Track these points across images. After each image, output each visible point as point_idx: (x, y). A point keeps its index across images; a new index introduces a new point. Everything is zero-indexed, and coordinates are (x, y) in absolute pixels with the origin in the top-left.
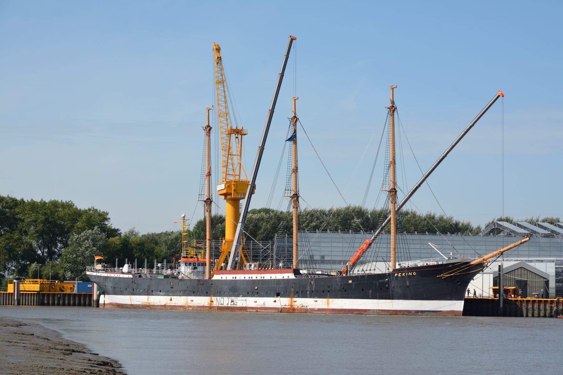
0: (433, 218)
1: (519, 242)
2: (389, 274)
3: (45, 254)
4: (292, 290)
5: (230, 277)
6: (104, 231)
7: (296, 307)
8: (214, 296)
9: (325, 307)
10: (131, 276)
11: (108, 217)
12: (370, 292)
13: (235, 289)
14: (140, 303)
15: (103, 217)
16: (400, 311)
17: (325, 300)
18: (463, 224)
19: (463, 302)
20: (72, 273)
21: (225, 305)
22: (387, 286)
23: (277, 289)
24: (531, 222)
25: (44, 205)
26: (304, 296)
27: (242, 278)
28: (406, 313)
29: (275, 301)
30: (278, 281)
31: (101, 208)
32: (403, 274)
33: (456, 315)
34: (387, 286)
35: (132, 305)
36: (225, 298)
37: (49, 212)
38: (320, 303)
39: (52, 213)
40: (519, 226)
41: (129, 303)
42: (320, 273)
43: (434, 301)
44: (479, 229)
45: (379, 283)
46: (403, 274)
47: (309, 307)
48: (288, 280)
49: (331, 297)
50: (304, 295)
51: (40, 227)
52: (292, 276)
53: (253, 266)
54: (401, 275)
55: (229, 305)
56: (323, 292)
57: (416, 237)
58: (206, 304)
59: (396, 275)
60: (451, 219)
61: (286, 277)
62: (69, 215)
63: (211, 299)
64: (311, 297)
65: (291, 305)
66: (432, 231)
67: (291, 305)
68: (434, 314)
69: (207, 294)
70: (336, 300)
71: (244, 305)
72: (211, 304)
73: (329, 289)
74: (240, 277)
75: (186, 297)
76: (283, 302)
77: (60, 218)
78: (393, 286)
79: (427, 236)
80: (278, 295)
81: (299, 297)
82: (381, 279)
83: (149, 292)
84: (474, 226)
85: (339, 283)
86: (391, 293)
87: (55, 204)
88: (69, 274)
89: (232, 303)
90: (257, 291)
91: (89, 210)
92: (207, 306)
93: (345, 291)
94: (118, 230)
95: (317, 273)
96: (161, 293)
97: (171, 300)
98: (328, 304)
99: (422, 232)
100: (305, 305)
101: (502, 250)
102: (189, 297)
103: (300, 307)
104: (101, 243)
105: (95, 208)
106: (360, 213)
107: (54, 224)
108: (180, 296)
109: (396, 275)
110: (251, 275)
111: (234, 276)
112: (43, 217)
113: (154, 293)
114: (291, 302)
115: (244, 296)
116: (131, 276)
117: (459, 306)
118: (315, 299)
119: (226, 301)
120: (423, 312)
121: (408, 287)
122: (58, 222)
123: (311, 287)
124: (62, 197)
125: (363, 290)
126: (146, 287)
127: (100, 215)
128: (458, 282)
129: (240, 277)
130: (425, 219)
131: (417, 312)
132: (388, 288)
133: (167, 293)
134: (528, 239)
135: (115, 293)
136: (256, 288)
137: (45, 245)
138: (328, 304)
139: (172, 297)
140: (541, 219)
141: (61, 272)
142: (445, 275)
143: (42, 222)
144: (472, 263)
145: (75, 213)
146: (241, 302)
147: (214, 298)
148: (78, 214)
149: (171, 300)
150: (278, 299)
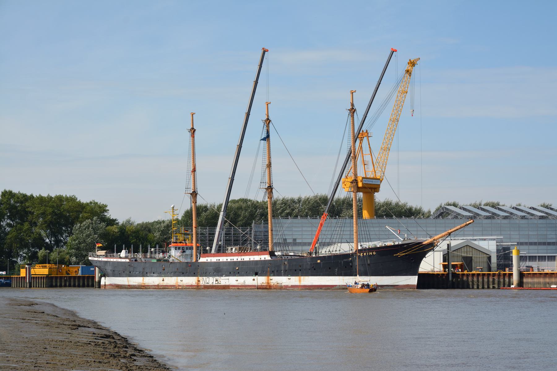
0: (391, 204)
1: (465, 224)
2: (352, 254)
3: (52, 242)
5: (214, 259)
6: (104, 221)
7: (272, 284)
8: (201, 276)
9: (297, 283)
10: (128, 260)
11: (107, 208)
13: (218, 270)
14: (137, 284)
15: (103, 209)
18: (416, 209)
20: (76, 258)
21: (210, 284)
22: (351, 264)
24: (475, 206)
25: (51, 200)
26: (279, 274)
27: (225, 260)
29: (254, 280)
30: (256, 262)
31: (101, 201)
32: (365, 254)
35: (129, 285)
36: (211, 278)
39: (59, 207)
40: (464, 209)
41: (127, 283)
42: (292, 254)
43: (392, 277)
45: (344, 262)
46: (365, 254)
47: (283, 284)
48: (265, 261)
50: (278, 273)
52: (268, 257)
53: (234, 249)
54: (363, 254)
55: (214, 284)
61: (263, 259)
64: (285, 275)
65: (268, 283)
66: (389, 216)
67: (268, 283)
68: (392, 288)
69: (194, 275)
70: (307, 277)
71: (227, 284)
73: (300, 268)
74: (223, 259)
76: (261, 280)
77: (64, 210)
79: (385, 220)
80: (256, 274)
81: (274, 276)
84: (425, 209)
87: (60, 199)
88: (74, 259)
91: (91, 203)
94: (115, 220)
95: (290, 254)
96: (154, 275)
97: (163, 280)
98: (300, 281)
101: (450, 231)
103: (276, 284)
105: (96, 201)
107: (61, 216)
110: (232, 258)
111: (218, 258)
114: (268, 280)
116: (128, 260)
117: (413, 280)
118: (289, 277)
119: (211, 281)
121: (369, 265)
124: (66, 192)
125: (330, 268)
126: (141, 270)
127: (100, 207)
128: (412, 260)
129: (223, 259)
132: (351, 267)
133: (160, 275)
134: (472, 221)
135: (114, 275)
137: (53, 234)
138: (300, 281)
139: (164, 278)
140: (483, 203)
143: (50, 214)
144: (424, 243)
146: (224, 281)
147: (200, 278)
148: (82, 207)
149: (163, 280)
150: (255, 278)
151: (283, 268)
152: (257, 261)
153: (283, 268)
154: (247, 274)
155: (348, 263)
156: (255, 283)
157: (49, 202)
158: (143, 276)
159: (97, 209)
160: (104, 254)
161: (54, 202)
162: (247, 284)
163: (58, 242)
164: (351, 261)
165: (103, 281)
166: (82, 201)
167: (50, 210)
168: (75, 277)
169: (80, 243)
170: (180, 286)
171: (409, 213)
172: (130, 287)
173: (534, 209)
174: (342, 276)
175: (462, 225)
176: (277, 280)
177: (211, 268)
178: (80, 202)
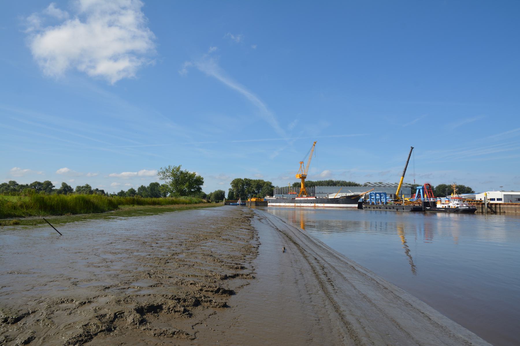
13: (301, 202)
15: (271, 183)
31: (270, 181)
38: (322, 205)
50: (318, 203)
57: (345, 187)
66: (350, 186)
74: (302, 199)
76: (313, 205)
83: (280, 202)
84: (361, 184)
87: (259, 180)
99: (347, 186)
106: (332, 181)
117: (357, 205)
119: (299, 205)
124: (261, 179)
129: (302, 199)
133: (284, 203)
137: (257, 190)
146: (302, 205)
148: (264, 183)
154: (309, 203)
163: (259, 192)
171: (356, 185)
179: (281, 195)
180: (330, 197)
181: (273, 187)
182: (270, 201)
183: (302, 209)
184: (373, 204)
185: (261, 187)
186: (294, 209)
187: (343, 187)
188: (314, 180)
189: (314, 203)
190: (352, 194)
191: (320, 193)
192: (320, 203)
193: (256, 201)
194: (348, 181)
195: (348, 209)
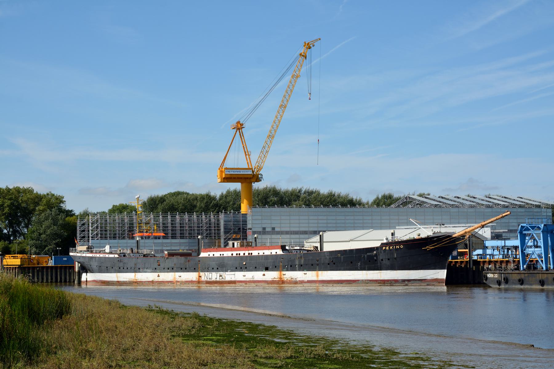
0: (334, 195)
1: (501, 216)
2: (377, 248)
3: (10, 233)
4: (281, 264)
5: (217, 254)
7: (285, 279)
8: (202, 272)
9: (315, 278)
10: (116, 256)
11: (64, 200)
12: (359, 264)
13: (222, 265)
14: (127, 280)
15: (60, 200)
16: (388, 281)
17: (314, 273)
18: (356, 200)
19: (446, 270)
20: (37, 248)
21: (214, 279)
22: (375, 258)
23: (266, 264)
24: (420, 195)
25: (9, 192)
28: (393, 282)
29: (264, 275)
30: (267, 257)
31: (57, 192)
32: (391, 248)
33: (439, 283)
34: (375, 258)
35: (118, 282)
36: (214, 273)
37: (13, 196)
38: (311, 275)
39: (17, 199)
40: (435, 200)
41: (115, 279)
42: (298, 248)
43: (419, 271)
44: (368, 203)
45: (368, 256)
46: (391, 248)
47: (298, 279)
48: (277, 256)
49: (320, 270)
50: (292, 268)
51: (6, 210)
52: (280, 252)
53: (236, 244)
54: (389, 248)
55: (218, 280)
56: (312, 265)
57: (322, 209)
58: (194, 279)
59: (384, 248)
60: (347, 196)
61: (274, 253)
62: (31, 199)
63: (199, 274)
64: (299, 270)
65: (281, 278)
66: (308, 204)
67: (281, 278)
68: (420, 282)
69: (195, 270)
70: (325, 272)
71: (233, 279)
72: (199, 279)
73: (317, 263)
75: (173, 273)
76: (272, 275)
78: (381, 258)
79: (331, 209)
80: (267, 269)
81: (287, 270)
82: (369, 252)
83: (136, 270)
84: (364, 200)
85: (328, 257)
86: (379, 264)
88: (34, 250)
89: (221, 278)
90: (245, 266)
91: (48, 194)
92: (195, 281)
93: (334, 264)
94: (72, 211)
95: (296, 248)
96: (148, 270)
97: (159, 276)
98: (317, 276)
100: (294, 277)
101: (483, 223)
102: (176, 273)
103: (289, 279)
104: (61, 222)
105: (53, 193)
106: (275, 192)
107: (18, 207)
108: (167, 272)
109: (384, 248)
110: (238, 252)
111: (222, 253)
112: (9, 202)
113: (141, 270)
114: (281, 275)
115: (232, 271)
116: (116, 256)
117: (442, 274)
118: (305, 272)
119: (214, 276)
120: (409, 281)
121: (395, 258)
122: (24, 205)
123: (300, 261)
124: (23, 185)
125: (351, 263)
126: (133, 266)
127: (57, 199)
130: (328, 197)
131: (404, 281)
132: (376, 260)
133: (155, 270)
134: (509, 213)
135: (100, 271)
136: (244, 263)
137: (11, 225)
138: (317, 276)
139: (160, 274)
140: (416, 194)
141: (28, 248)
142: (429, 248)
143: (8, 206)
144: (454, 236)
145: (37, 197)
146: (229, 276)
147: (202, 274)
148: (38, 199)
149: (159, 276)
150: (266, 273)
151: (297, 263)
152: (267, 255)
153: (297, 263)
154: (256, 269)
155: (372, 257)
156: (264, 278)
157: (6, 195)
158: (135, 271)
159: (53, 200)
160: (85, 249)
161: (12, 193)
162: (256, 279)
164: (376, 255)
165: (84, 277)
166: (39, 193)
167: (8, 203)
168: (43, 267)
169: (40, 234)
170: (178, 282)
171: (351, 203)
172: (119, 283)
173: (442, 198)
174: (365, 270)
175: (498, 217)
176: (289, 275)
177: (213, 264)
178: (37, 193)
179: (132, 243)
180: (328, 247)
181: (69, 213)
182: (94, 265)
183: (222, 289)
184: (532, 266)
185: (27, 213)
186: (196, 293)
187: (313, 209)
188: (285, 185)
189: (275, 268)
190: (426, 232)
191: (264, 232)
192: (302, 267)
193: (22, 269)
194: (324, 190)
195: (412, 288)
